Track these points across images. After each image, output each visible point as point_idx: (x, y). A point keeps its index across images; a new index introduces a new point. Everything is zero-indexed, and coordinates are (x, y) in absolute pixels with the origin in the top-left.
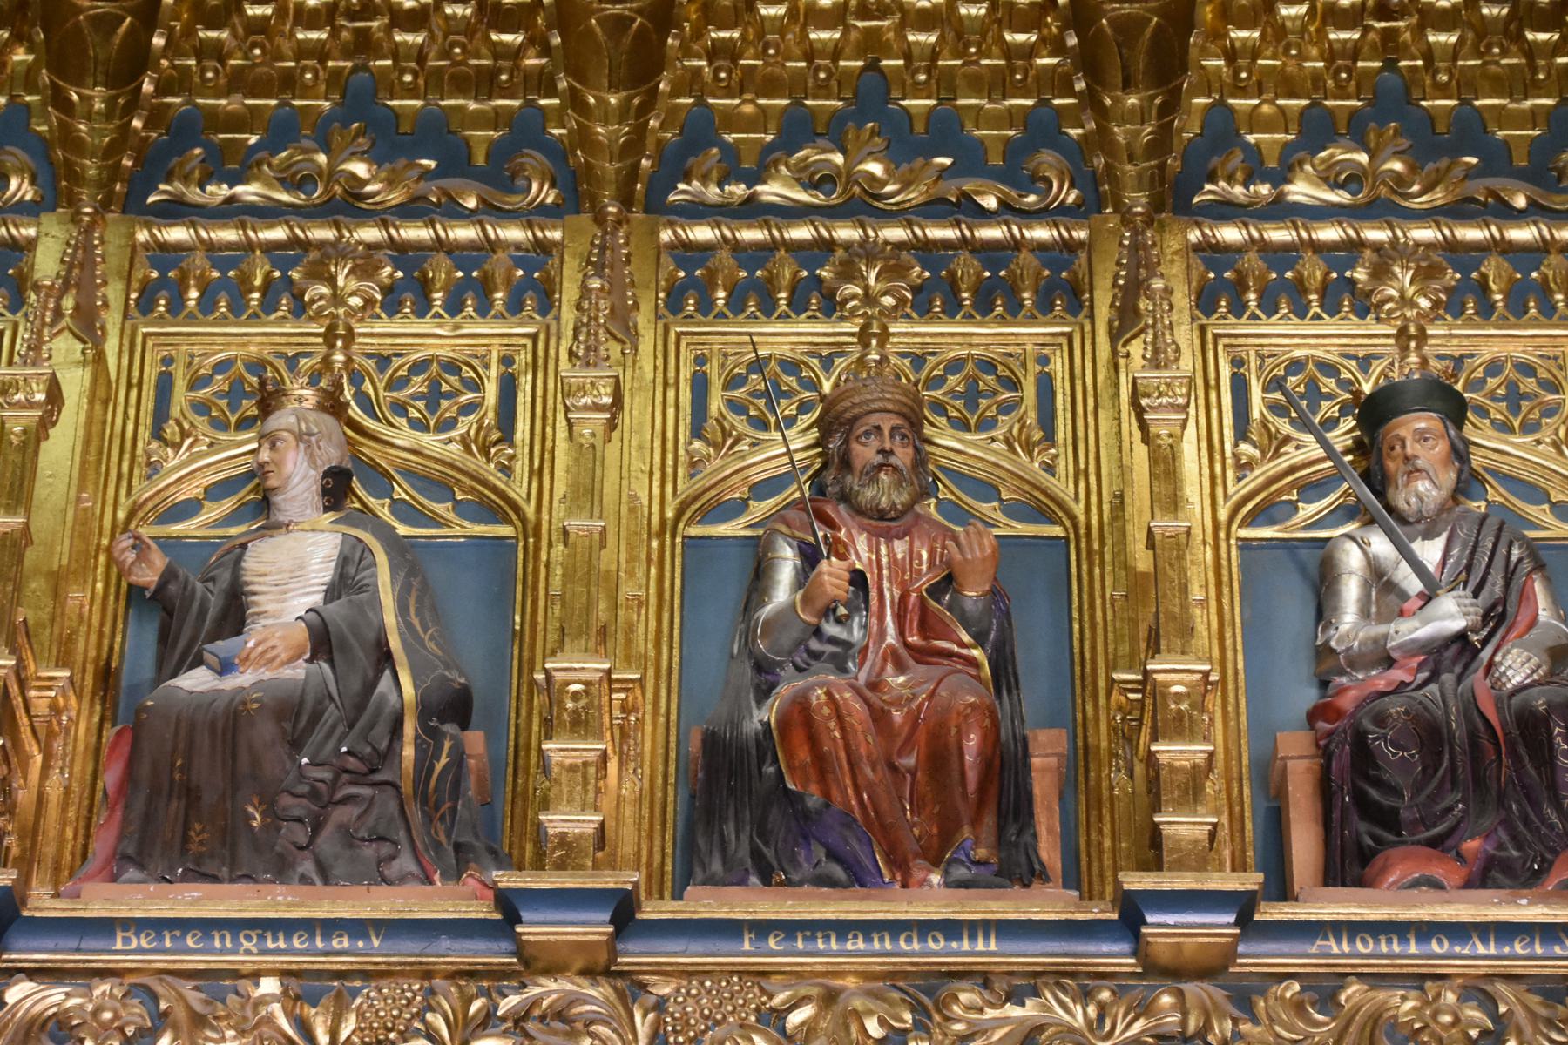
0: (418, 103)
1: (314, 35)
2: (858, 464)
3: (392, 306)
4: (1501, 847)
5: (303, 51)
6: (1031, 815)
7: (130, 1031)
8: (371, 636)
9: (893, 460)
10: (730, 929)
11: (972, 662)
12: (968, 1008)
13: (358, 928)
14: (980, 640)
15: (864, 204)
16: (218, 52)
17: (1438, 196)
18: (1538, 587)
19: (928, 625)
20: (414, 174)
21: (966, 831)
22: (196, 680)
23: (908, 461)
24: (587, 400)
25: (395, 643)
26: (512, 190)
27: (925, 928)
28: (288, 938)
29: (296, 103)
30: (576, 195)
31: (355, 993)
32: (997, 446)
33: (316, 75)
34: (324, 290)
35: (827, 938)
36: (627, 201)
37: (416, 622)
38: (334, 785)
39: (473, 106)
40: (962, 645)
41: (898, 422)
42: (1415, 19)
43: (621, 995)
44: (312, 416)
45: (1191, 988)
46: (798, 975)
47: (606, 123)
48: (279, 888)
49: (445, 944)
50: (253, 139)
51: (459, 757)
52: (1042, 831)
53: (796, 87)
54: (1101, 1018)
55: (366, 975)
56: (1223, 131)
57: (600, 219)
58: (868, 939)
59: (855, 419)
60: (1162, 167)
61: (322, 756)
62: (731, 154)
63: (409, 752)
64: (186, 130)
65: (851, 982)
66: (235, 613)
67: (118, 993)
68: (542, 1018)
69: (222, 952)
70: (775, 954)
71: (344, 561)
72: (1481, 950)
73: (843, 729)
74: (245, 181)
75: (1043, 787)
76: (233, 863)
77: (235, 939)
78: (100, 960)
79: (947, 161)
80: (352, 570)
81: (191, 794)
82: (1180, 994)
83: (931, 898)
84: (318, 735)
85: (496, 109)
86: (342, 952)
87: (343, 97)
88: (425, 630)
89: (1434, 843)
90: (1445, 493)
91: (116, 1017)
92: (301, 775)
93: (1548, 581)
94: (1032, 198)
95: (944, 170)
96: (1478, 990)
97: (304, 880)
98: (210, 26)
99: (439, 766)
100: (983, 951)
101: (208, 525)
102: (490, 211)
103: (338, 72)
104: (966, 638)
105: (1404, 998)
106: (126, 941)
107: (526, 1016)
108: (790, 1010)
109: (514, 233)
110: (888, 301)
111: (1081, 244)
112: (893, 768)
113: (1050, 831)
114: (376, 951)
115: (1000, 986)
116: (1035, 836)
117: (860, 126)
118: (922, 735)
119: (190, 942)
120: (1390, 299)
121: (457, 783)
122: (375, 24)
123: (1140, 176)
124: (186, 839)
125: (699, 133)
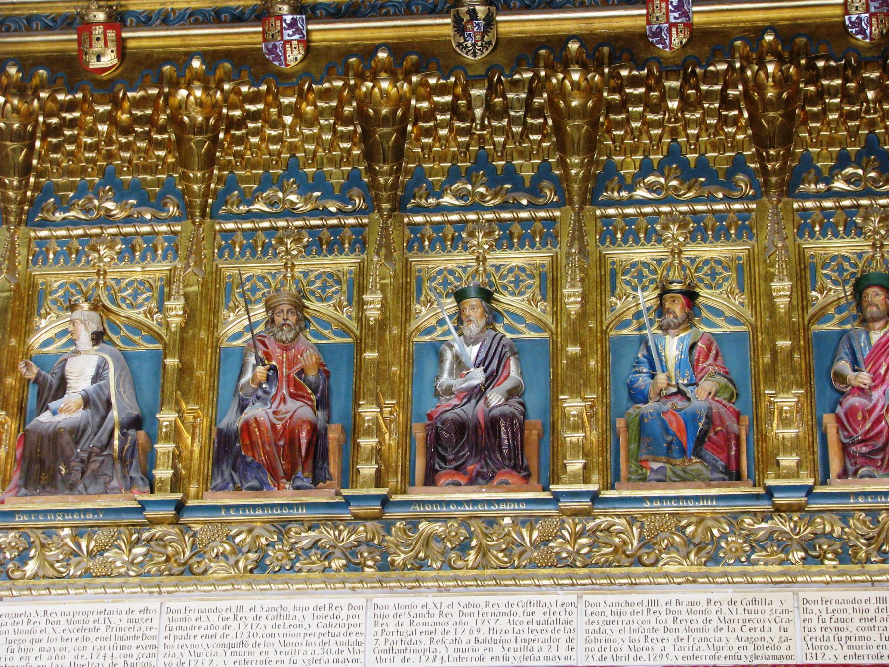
0: (130, 178)
1: (91, 155)
2: (277, 323)
3: (121, 258)
4: (482, 468)
5: (88, 160)
6: (328, 456)
7: (21, 549)
8: (105, 398)
9: (288, 322)
10: (217, 508)
11: (311, 400)
12: (296, 533)
13: (95, 511)
14: (315, 392)
15: (290, 213)
16: (57, 163)
17: (497, 201)
18: (512, 362)
19: (297, 386)
20: (128, 206)
21: (300, 469)
22: (45, 417)
23: (294, 321)
24: (174, 313)
25: (113, 401)
26: (164, 211)
27: (281, 506)
28: (72, 516)
29: (87, 179)
30: (187, 212)
31: (95, 533)
32: (330, 309)
33: (93, 169)
34: (97, 255)
35: (249, 510)
36: (203, 215)
37: (122, 390)
38: (89, 458)
39: (149, 178)
40: (307, 393)
41: (290, 307)
42: (490, 130)
43: (181, 531)
44: (87, 313)
45: (369, 524)
46: (241, 523)
47: (197, 183)
48: (70, 497)
49: (124, 516)
50: (71, 194)
51: (135, 444)
52: (332, 462)
53: (266, 166)
54: (340, 535)
55: (99, 527)
56: (419, 177)
57: (194, 223)
58: (263, 510)
59: (275, 307)
60: (396, 193)
61: (85, 448)
62: (242, 192)
63: (116, 442)
64: (47, 191)
65: (259, 524)
66: (61, 388)
67: (17, 536)
68: (156, 540)
69: (51, 520)
70: (233, 516)
71: (98, 367)
72: (467, 508)
73: (259, 431)
74: (69, 211)
75: (333, 446)
76: (56, 489)
77: (55, 516)
78: (12, 525)
79: (319, 194)
80: (101, 371)
81: (42, 462)
82: (365, 526)
83: (285, 495)
84: (83, 441)
85: (158, 179)
86: (90, 519)
87: (104, 175)
88: (125, 392)
89: (457, 469)
90: (479, 329)
91: (17, 544)
92: (77, 456)
93: (518, 360)
94: (350, 207)
95: (317, 197)
96: (465, 522)
97: (80, 493)
98: (54, 152)
99: (126, 447)
100: (302, 513)
101: (57, 348)
102: (157, 220)
103: (101, 166)
104: (309, 391)
105: (440, 526)
106: (19, 518)
107: (151, 539)
108: (237, 535)
109: (164, 228)
110: (295, 253)
111: (366, 225)
112: (277, 445)
113: (334, 461)
114: (101, 519)
115: (306, 525)
116: (328, 464)
117: (288, 180)
118: (287, 432)
119: (40, 518)
120: (474, 245)
121: (133, 452)
122: (113, 148)
123: (389, 196)
124: (40, 479)
125: (231, 184)
